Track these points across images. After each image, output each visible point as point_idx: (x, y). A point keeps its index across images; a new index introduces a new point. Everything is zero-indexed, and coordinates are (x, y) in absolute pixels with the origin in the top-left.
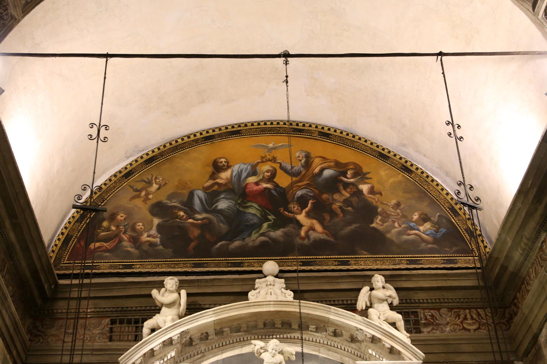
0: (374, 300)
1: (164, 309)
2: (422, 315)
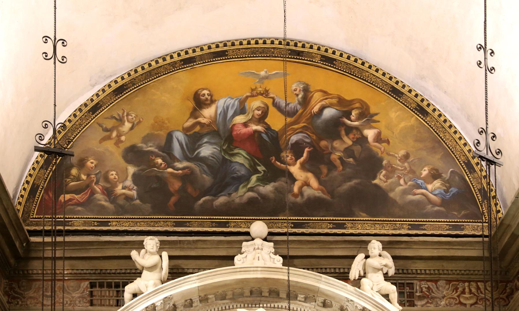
0: (368, 270)
1: (145, 273)
2: (418, 287)
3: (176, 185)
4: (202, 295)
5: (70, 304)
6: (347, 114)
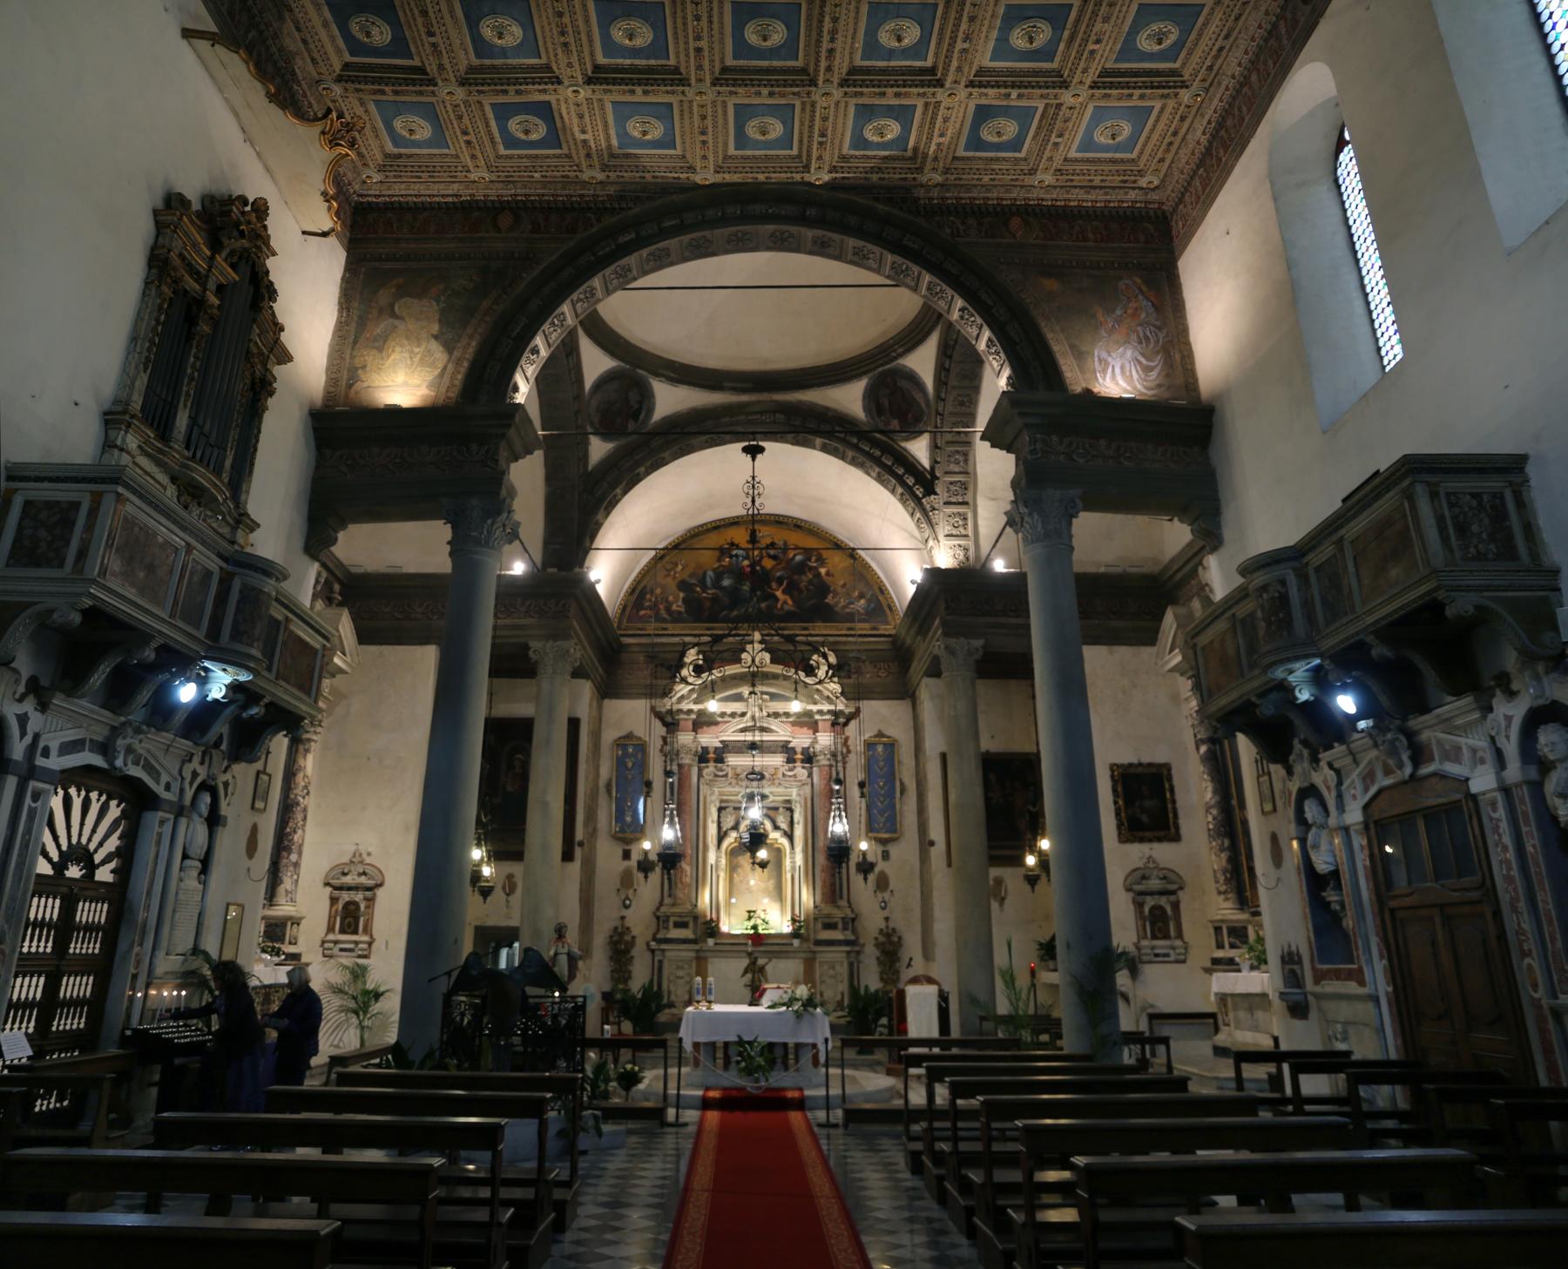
3: (708, 604)
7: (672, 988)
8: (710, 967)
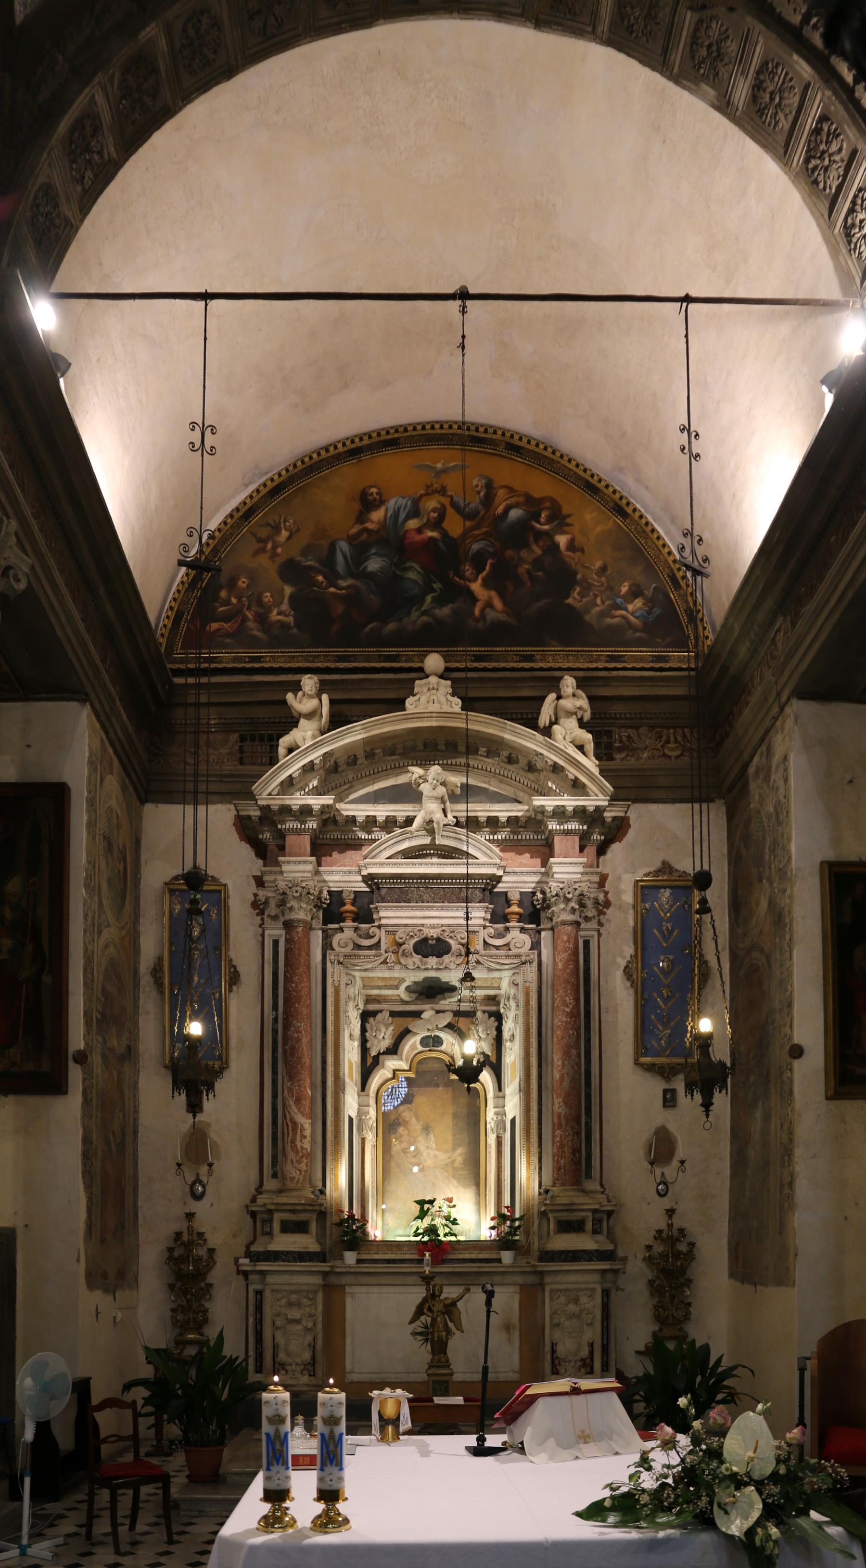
0: (561, 714)
1: (302, 722)
3: (339, 608)
4: (368, 749)
5: (217, 763)
6: (536, 517)
7: (280, 1340)
8: (349, 1301)
